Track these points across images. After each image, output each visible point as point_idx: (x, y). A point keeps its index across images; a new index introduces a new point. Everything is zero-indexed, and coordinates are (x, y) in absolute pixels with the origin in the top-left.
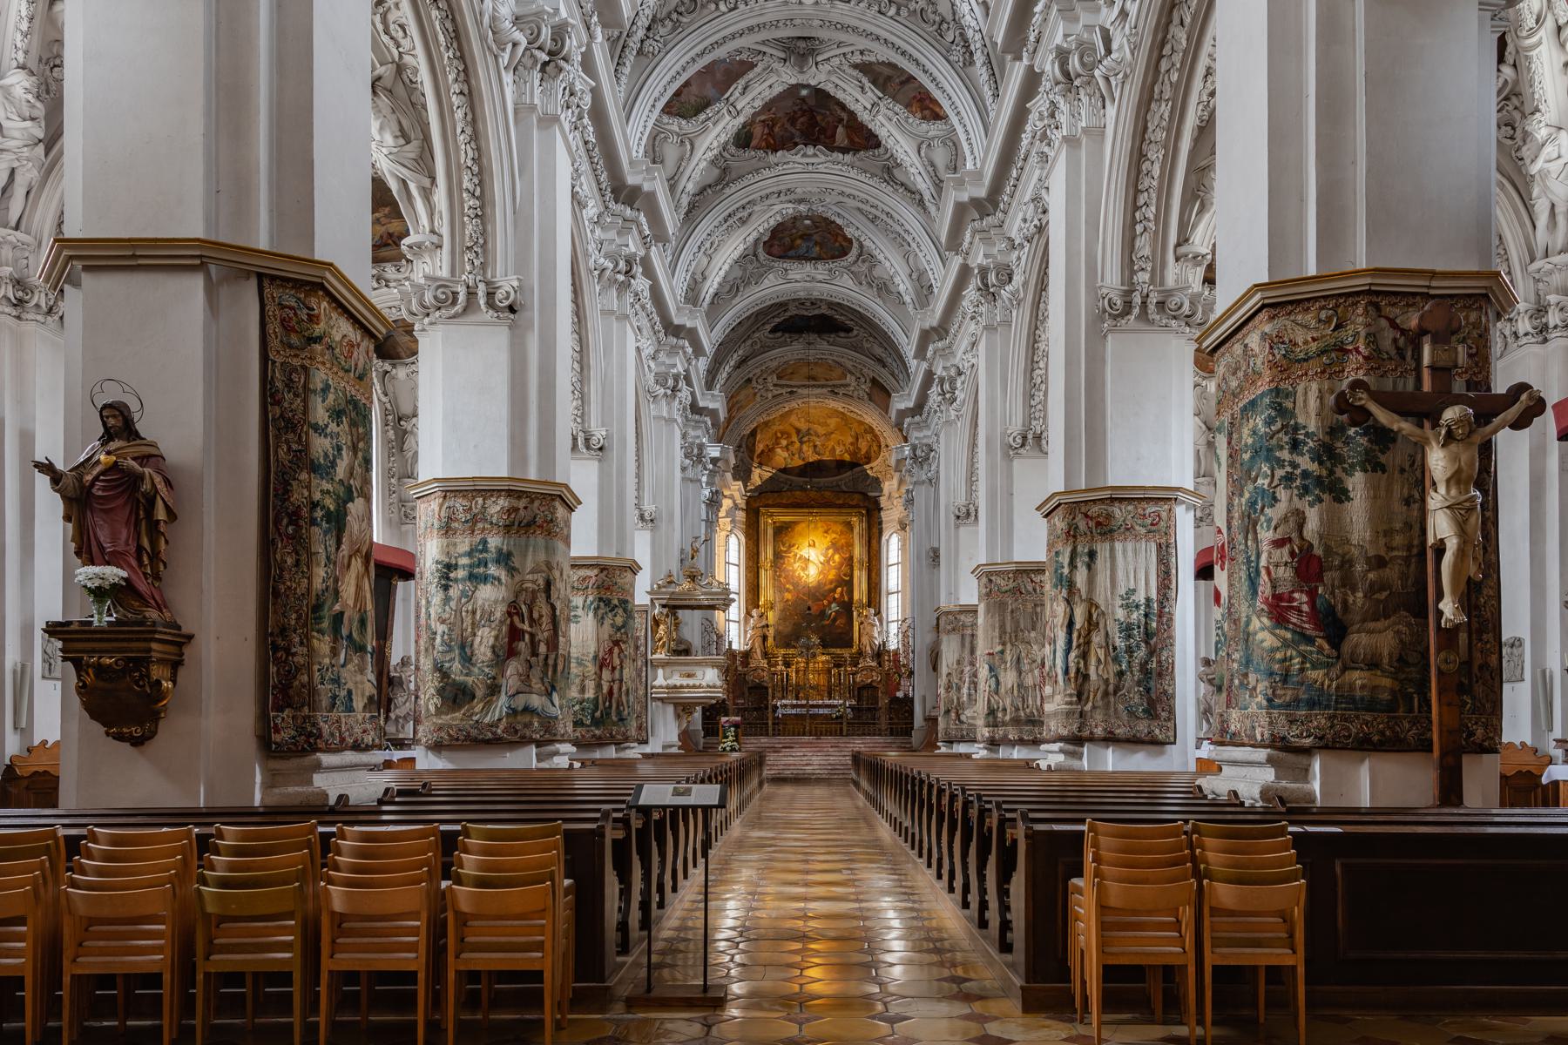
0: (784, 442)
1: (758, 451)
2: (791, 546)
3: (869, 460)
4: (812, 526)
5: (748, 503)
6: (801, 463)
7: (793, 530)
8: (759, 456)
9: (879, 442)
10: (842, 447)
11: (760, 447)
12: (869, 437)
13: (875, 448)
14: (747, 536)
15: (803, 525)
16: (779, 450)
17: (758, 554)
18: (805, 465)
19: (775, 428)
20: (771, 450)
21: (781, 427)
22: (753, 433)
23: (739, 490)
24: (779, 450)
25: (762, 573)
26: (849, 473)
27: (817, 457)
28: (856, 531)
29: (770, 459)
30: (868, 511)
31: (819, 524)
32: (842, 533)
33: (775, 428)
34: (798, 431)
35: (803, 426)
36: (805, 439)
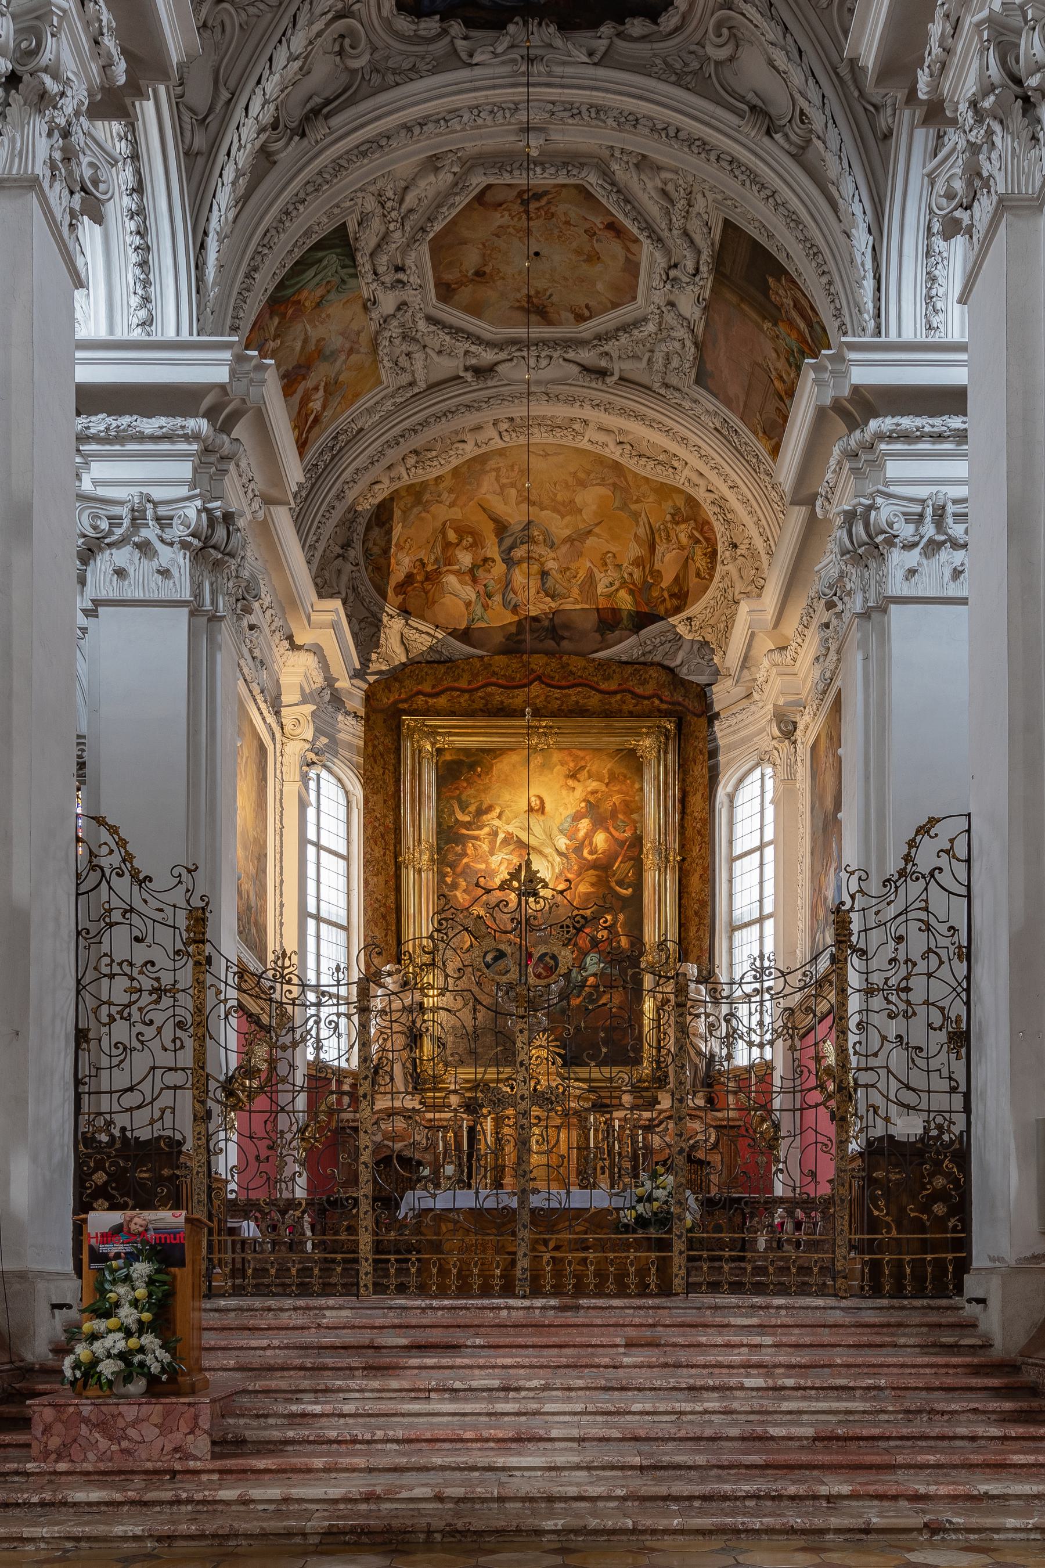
0: (465, 559)
1: (398, 575)
2: (480, 812)
3: (681, 598)
4: (537, 760)
5: (369, 697)
6: (510, 618)
7: (488, 770)
8: (402, 587)
9: (711, 542)
10: (613, 573)
11: (402, 564)
12: (683, 533)
13: (700, 562)
14: (368, 782)
15: (514, 758)
16: (451, 580)
17: (397, 830)
18: (519, 623)
19: (442, 512)
20: (432, 577)
21: (456, 513)
22: (382, 515)
23: (335, 626)
24: (451, 580)
25: (409, 877)
26: (632, 640)
27: (548, 605)
28: (649, 775)
29: (430, 602)
30: (679, 726)
31: (556, 757)
32: (613, 777)
33: (442, 512)
34: (501, 528)
35: (514, 514)
36: (519, 553)
